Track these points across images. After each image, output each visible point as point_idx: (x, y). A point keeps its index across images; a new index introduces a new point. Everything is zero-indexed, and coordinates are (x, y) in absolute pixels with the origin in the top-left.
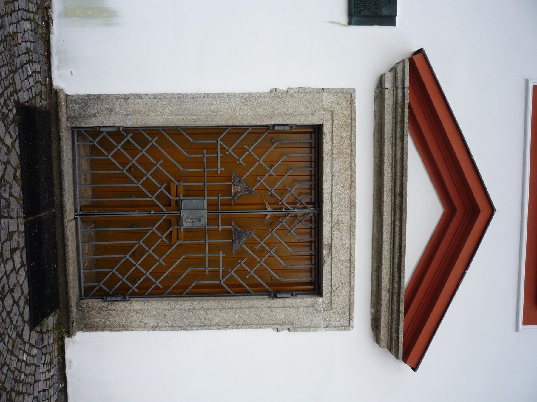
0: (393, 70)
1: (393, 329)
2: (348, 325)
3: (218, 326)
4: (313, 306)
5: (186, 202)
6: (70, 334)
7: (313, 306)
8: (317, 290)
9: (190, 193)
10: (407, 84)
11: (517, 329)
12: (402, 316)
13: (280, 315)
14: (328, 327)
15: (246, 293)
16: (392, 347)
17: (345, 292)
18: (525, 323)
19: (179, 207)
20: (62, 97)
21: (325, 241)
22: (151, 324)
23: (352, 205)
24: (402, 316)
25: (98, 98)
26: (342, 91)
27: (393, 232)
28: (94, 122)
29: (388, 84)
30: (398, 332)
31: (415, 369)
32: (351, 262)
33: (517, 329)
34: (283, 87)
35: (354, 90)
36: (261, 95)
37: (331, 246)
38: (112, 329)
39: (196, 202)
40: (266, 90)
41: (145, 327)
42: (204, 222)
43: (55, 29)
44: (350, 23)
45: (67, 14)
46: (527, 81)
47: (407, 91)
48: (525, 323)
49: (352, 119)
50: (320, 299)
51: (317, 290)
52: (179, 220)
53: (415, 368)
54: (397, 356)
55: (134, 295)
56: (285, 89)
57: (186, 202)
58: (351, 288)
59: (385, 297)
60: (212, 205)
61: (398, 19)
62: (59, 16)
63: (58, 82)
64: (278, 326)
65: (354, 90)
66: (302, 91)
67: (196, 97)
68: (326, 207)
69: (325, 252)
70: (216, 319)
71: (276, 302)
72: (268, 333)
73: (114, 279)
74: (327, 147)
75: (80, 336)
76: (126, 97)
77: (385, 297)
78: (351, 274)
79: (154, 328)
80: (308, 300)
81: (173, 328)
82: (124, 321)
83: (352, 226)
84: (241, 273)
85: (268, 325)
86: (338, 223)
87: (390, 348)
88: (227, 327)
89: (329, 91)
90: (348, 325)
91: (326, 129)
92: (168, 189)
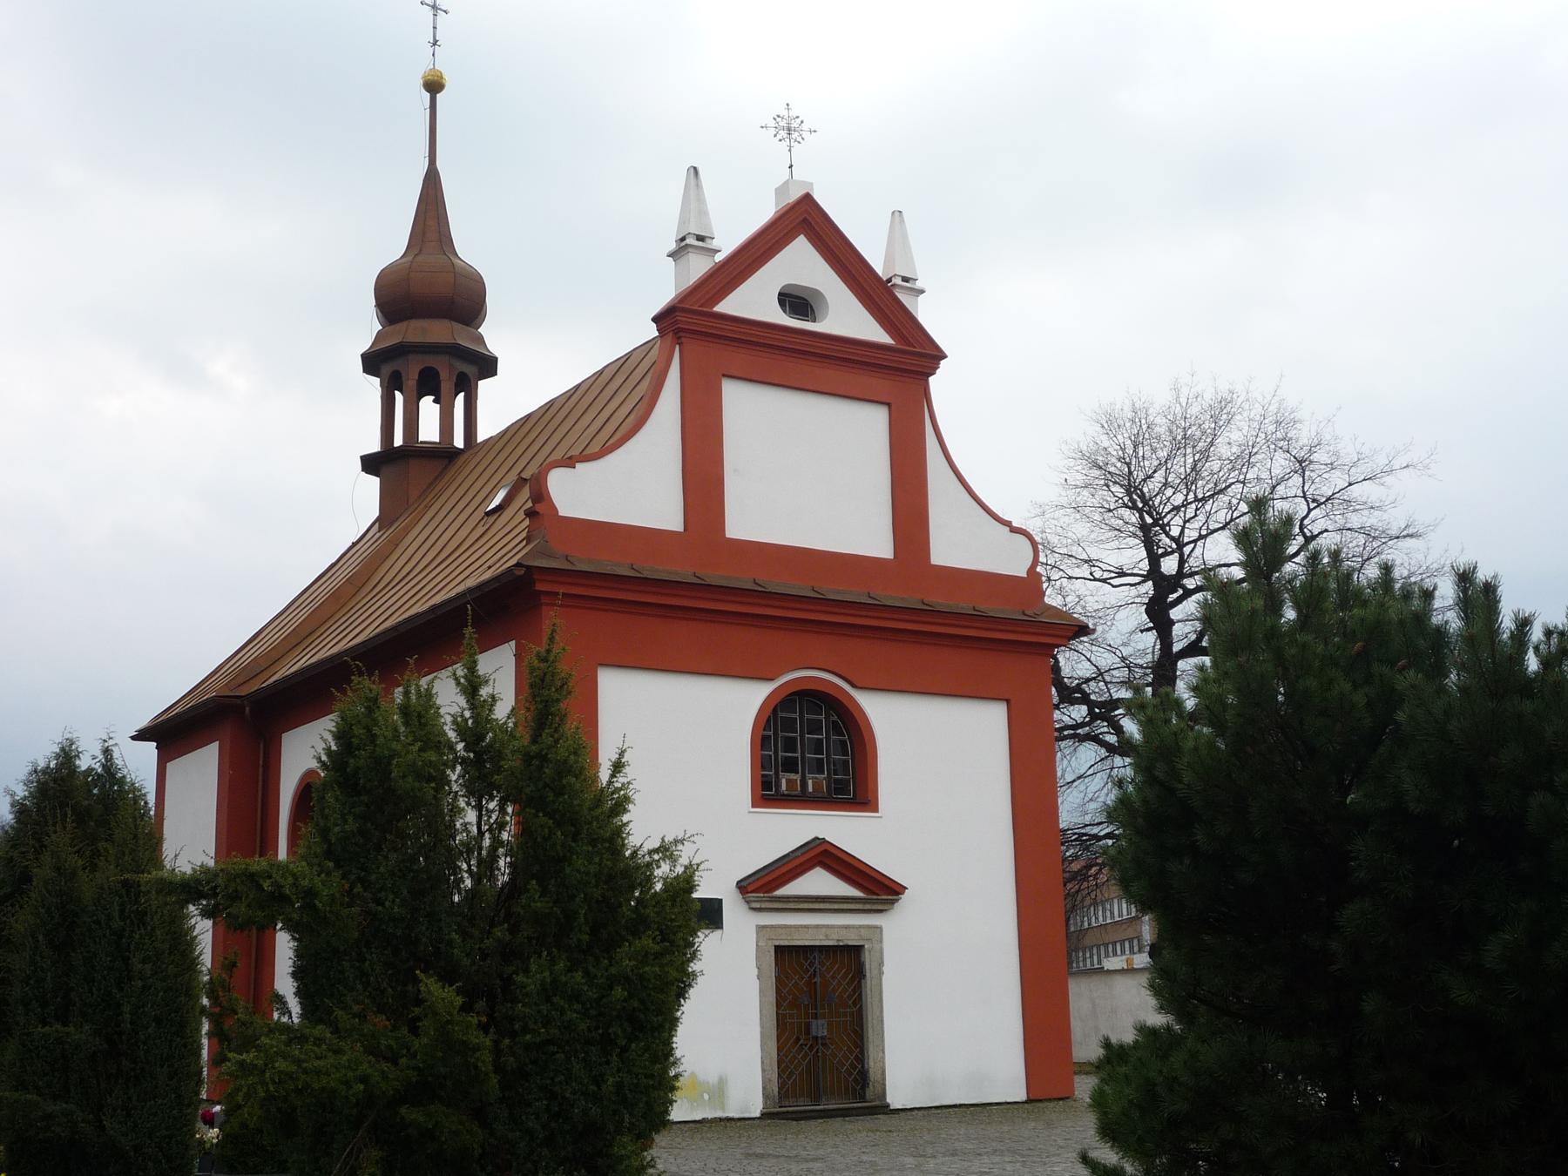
0: (748, 902)
2: (880, 928)
3: (882, 1012)
4: (870, 952)
5: (814, 1034)
6: (888, 1106)
7: (870, 952)
9: (808, 1031)
10: (762, 895)
11: (880, 817)
12: (879, 897)
13: (875, 972)
14: (881, 942)
15: (860, 995)
16: (893, 902)
17: (862, 930)
20: (765, 1110)
21: (836, 944)
22: (881, 1054)
23: (817, 927)
24: (879, 897)
25: (764, 1088)
28: (776, 1090)
29: (757, 905)
31: (907, 888)
32: (847, 927)
33: (880, 817)
34: (756, 971)
35: (757, 926)
37: (838, 940)
38: (884, 1079)
41: (883, 1058)
42: (823, 1021)
43: (731, 1115)
44: (722, 928)
45: (723, 1109)
46: (750, 812)
47: (766, 895)
49: (772, 926)
50: (866, 946)
52: (822, 1038)
53: (906, 888)
54: (897, 900)
55: (863, 1067)
56: (756, 970)
58: (860, 927)
59: (868, 907)
60: (816, 1016)
62: (724, 1112)
63: (757, 1114)
64: (881, 973)
65: (757, 926)
66: (758, 958)
67: (762, 1026)
68: (817, 943)
69: (841, 944)
70: (878, 1013)
72: (884, 978)
73: (856, 1080)
74: (786, 943)
75: (889, 1100)
76: (763, 1070)
77: (868, 907)
78: (853, 927)
79: (884, 1053)
80: (867, 953)
81: (883, 1041)
83: (827, 927)
84: (850, 997)
85: (881, 980)
86: (826, 936)
87: (893, 903)
90: (880, 928)
91: (777, 944)
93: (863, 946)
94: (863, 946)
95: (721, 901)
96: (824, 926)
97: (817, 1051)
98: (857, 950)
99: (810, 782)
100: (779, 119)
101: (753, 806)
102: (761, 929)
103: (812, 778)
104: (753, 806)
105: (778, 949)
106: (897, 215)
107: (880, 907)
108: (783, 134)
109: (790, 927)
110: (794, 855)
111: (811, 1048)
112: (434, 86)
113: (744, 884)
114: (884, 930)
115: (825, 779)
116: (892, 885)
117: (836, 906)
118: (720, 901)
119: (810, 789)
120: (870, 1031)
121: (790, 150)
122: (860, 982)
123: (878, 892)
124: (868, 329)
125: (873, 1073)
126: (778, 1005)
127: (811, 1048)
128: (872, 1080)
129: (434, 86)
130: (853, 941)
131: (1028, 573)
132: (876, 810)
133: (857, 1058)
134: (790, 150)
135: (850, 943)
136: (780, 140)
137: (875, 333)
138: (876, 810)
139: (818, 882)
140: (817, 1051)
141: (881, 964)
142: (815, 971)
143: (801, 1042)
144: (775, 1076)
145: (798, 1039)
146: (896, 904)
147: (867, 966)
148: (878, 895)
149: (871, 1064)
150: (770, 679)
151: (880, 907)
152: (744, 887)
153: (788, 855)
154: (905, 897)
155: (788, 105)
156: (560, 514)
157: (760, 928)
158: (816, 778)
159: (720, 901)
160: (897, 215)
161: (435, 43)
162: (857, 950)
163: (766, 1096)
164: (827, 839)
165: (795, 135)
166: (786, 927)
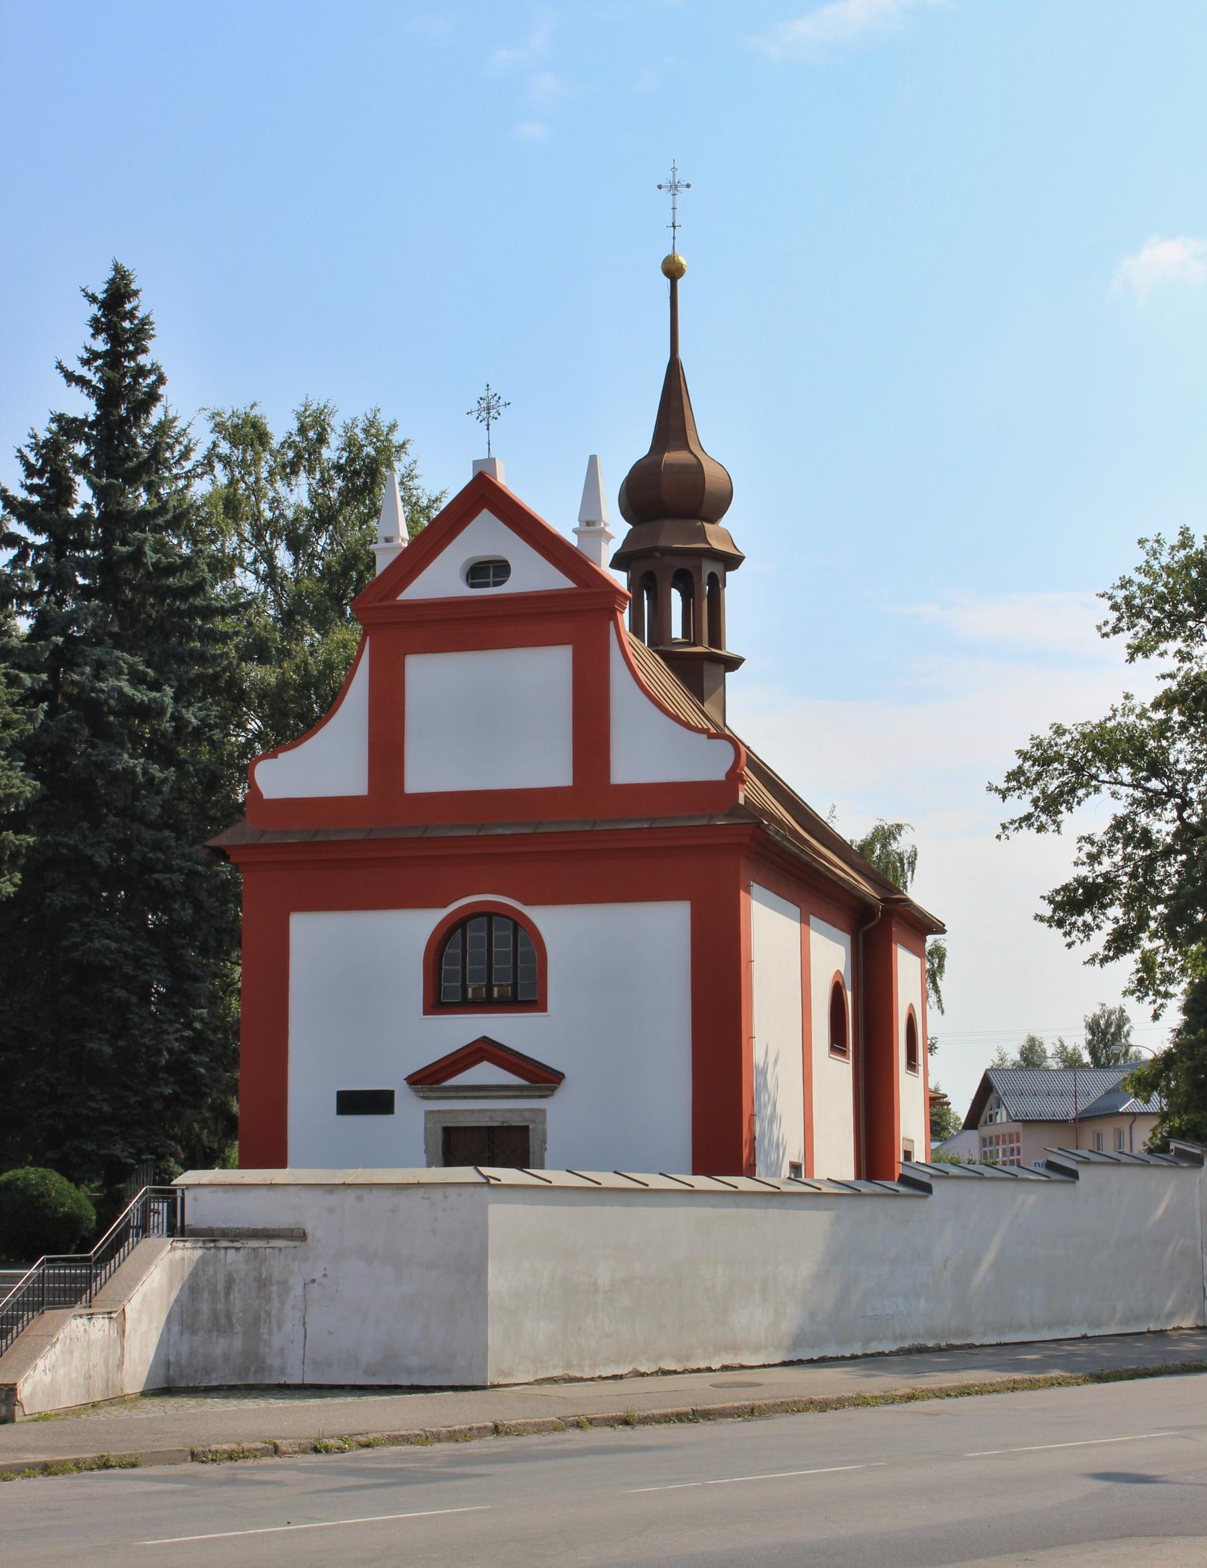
0: (415, 1092)
1: (541, 1089)
2: (542, 1112)
7: (533, 1130)
8: (526, 1128)
14: (544, 1122)
16: (554, 1089)
18: (546, 1011)
21: (501, 1125)
26: (425, 1117)
32: (511, 1111)
34: (424, 1147)
35: (426, 1111)
36: (427, 1158)
40: (425, 1156)
48: (546, 1011)
51: (526, 1128)
56: (424, 1147)
58: (524, 1110)
65: (426, 1111)
66: (426, 1137)
68: (483, 1124)
69: (505, 1125)
71: (531, 1150)
80: (531, 1133)
89: (426, 1124)
90: (542, 1112)
91: (445, 1125)
93: (528, 1126)
94: (528, 1126)
95: (393, 1091)
98: (525, 1130)
99: (496, 989)
100: (481, 402)
101: (424, 1014)
102: (429, 1113)
103: (497, 986)
104: (424, 1014)
105: (447, 1131)
106: (593, 460)
108: (484, 414)
112: (673, 271)
114: (547, 1113)
115: (508, 985)
119: (496, 995)
121: (488, 429)
124: (557, 581)
129: (673, 271)
130: (516, 1121)
131: (727, 775)
132: (545, 1010)
134: (488, 429)
136: (499, 414)
137: (557, 581)
138: (545, 1010)
139: (485, 1073)
141: (544, 1141)
150: (445, 906)
153: (453, 1054)
155: (488, 386)
156: (266, 796)
157: (429, 1113)
158: (502, 985)
160: (593, 460)
162: (525, 1130)
165: (493, 413)
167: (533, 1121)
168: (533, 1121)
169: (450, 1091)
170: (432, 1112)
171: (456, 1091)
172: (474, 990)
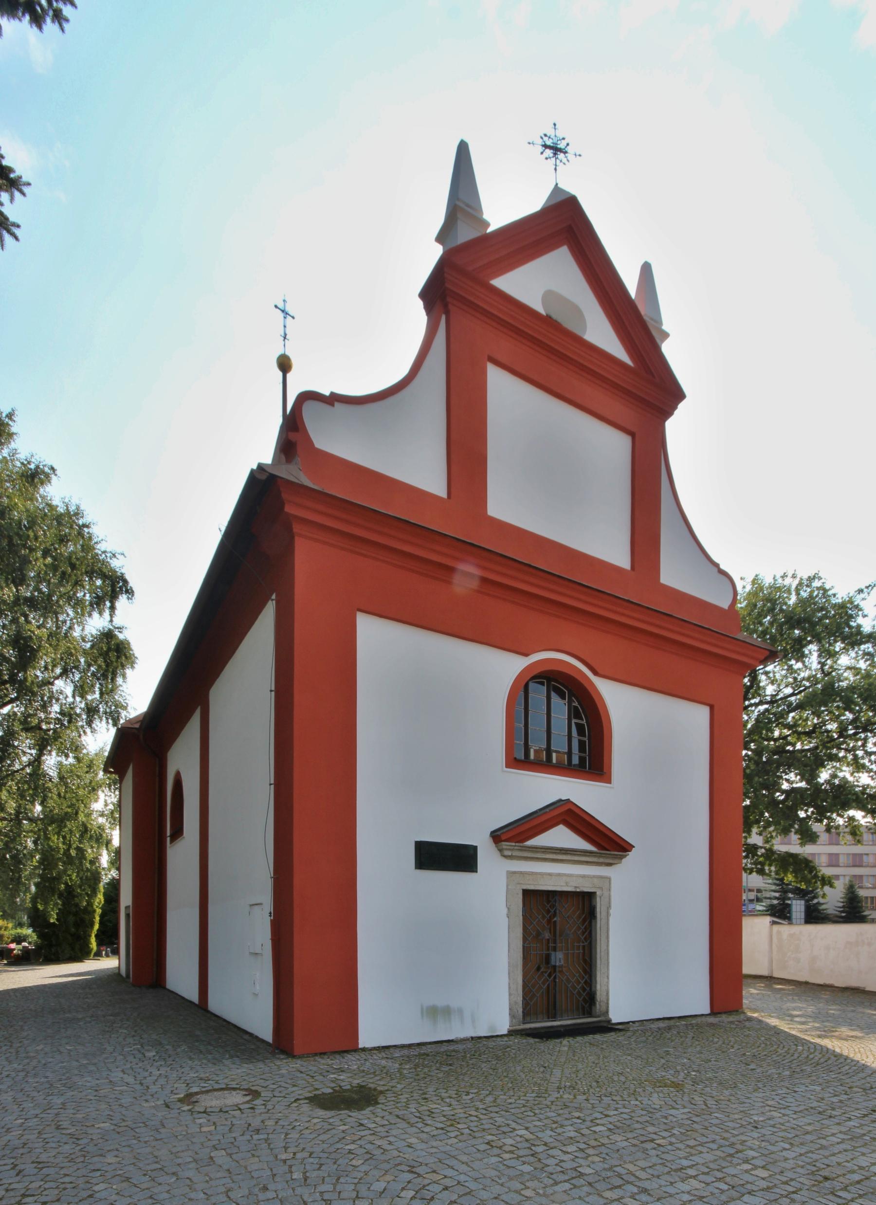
2: (610, 879)
3: (608, 946)
4: (600, 897)
5: (553, 963)
7: (600, 897)
10: (514, 844)
13: (604, 914)
16: (621, 858)
19: (554, 967)
22: (606, 980)
23: (559, 875)
25: (510, 1009)
26: (508, 878)
27: (575, 855)
28: (520, 1010)
30: (617, 855)
32: (584, 876)
34: (505, 911)
38: (608, 1000)
39: (553, 958)
40: (507, 919)
46: (503, 771)
47: (517, 844)
49: (521, 873)
50: (598, 893)
54: (626, 856)
55: (591, 989)
56: (506, 909)
57: (553, 963)
58: (594, 877)
59: (601, 860)
61: (475, 845)
64: (608, 915)
69: (578, 890)
73: (584, 1000)
76: (510, 995)
79: (608, 978)
80: (598, 899)
82: (605, 994)
87: (622, 859)
88: (608, 941)
91: (525, 887)
92: (546, 972)
93: (595, 893)
94: (595, 893)
96: (565, 875)
97: (555, 977)
102: (511, 874)
105: (527, 893)
107: (611, 861)
109: (536, 874)
110: (543, 812)
111: (550, 975)
113: (499, 833)
114: (612, 882)
116: (622, 843)
117: (576, 858)
118: (475, 848)
119: (554, 761)
120: (598, 961)
122: (590, 923)
123: (607, 847)
125: (600, 996)
126: (525, 939)
127: (550, 975)
128: (599, 1000)
132: (609, 781)
133: (586, 982)
135: (586, 890)
140: (555, 977)
141: (609, 907)
142: (555, 912)
143: (542, 970)
144: (520, 999)
145: (538, 969)
146: (624, 860)
147: (598, 910)
148: (608, 850)
149: (598, 987)
151: (611, 861)
152: (497, 837)
154: (631, 855)
157: (511, 874)
159: (475, 848)
161: (285, 335)
163: (512, 1016)
164: (572, 800)
166: (532, 873)
167: (601, 888)
168: (601, 888)
169: (537, 852)
170: (514, 873)
171: (543, 852)
172: (535, 751)
